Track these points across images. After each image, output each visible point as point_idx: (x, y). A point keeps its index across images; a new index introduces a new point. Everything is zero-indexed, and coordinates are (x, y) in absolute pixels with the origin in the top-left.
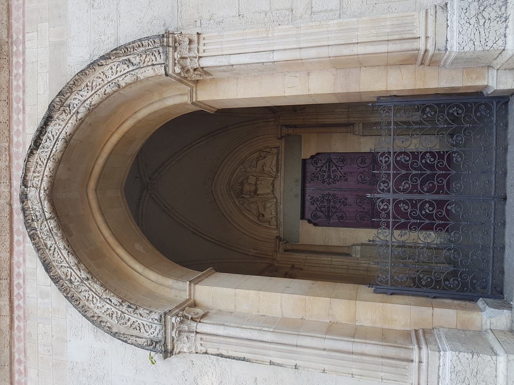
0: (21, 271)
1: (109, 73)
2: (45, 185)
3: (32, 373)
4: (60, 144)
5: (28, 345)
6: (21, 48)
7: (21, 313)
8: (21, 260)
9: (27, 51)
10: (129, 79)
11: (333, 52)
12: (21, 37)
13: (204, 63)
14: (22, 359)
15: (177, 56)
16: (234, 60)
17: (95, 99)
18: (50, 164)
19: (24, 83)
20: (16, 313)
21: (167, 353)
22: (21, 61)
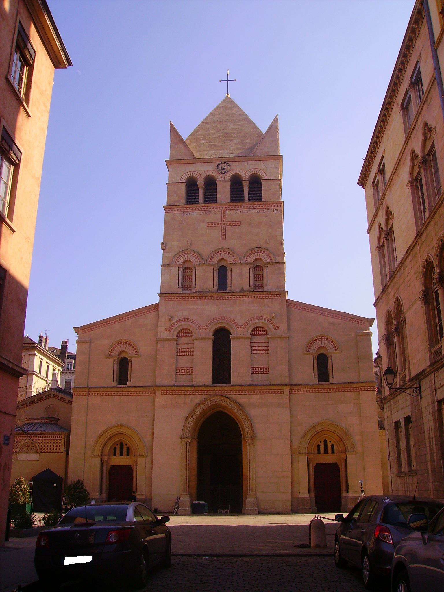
0: (197, 393)
1: (247, 422)
2: (220, 403)
3: (170, 397)
4: (230, 408)
5: (177, 396)
6: (256, 393)
7: (186, 393)
8: (200, 393)
9: (254, 395)
10: (245, 427)
11: (249, 476)
12: (258, 393)
13: (248, 447)
14: (173, 394)
15: (249, 440)
16: (248, 454)
17: (241, 418)
18: (225, 405)
19: (246, 394)
20: (186, 392)
21: (181, 438)
22: (252, 393)
